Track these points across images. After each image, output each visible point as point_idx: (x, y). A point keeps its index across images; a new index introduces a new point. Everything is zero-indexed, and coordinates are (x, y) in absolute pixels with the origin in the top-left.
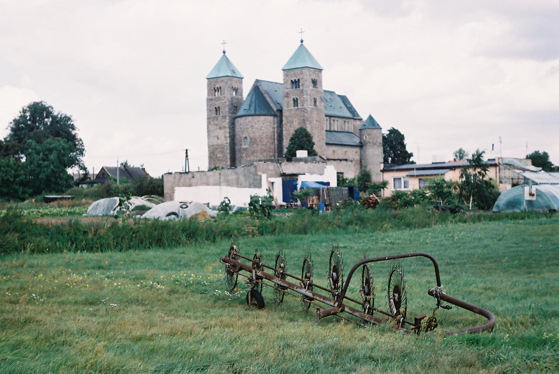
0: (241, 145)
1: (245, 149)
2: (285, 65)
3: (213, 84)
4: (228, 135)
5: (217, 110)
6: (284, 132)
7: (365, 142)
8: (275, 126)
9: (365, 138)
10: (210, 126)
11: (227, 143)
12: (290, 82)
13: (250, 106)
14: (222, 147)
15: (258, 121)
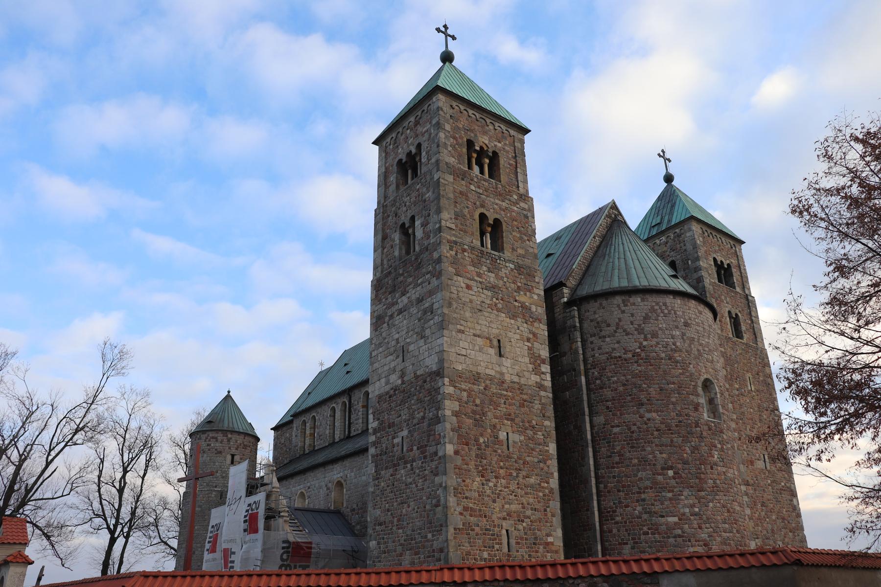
3: (463, 123)
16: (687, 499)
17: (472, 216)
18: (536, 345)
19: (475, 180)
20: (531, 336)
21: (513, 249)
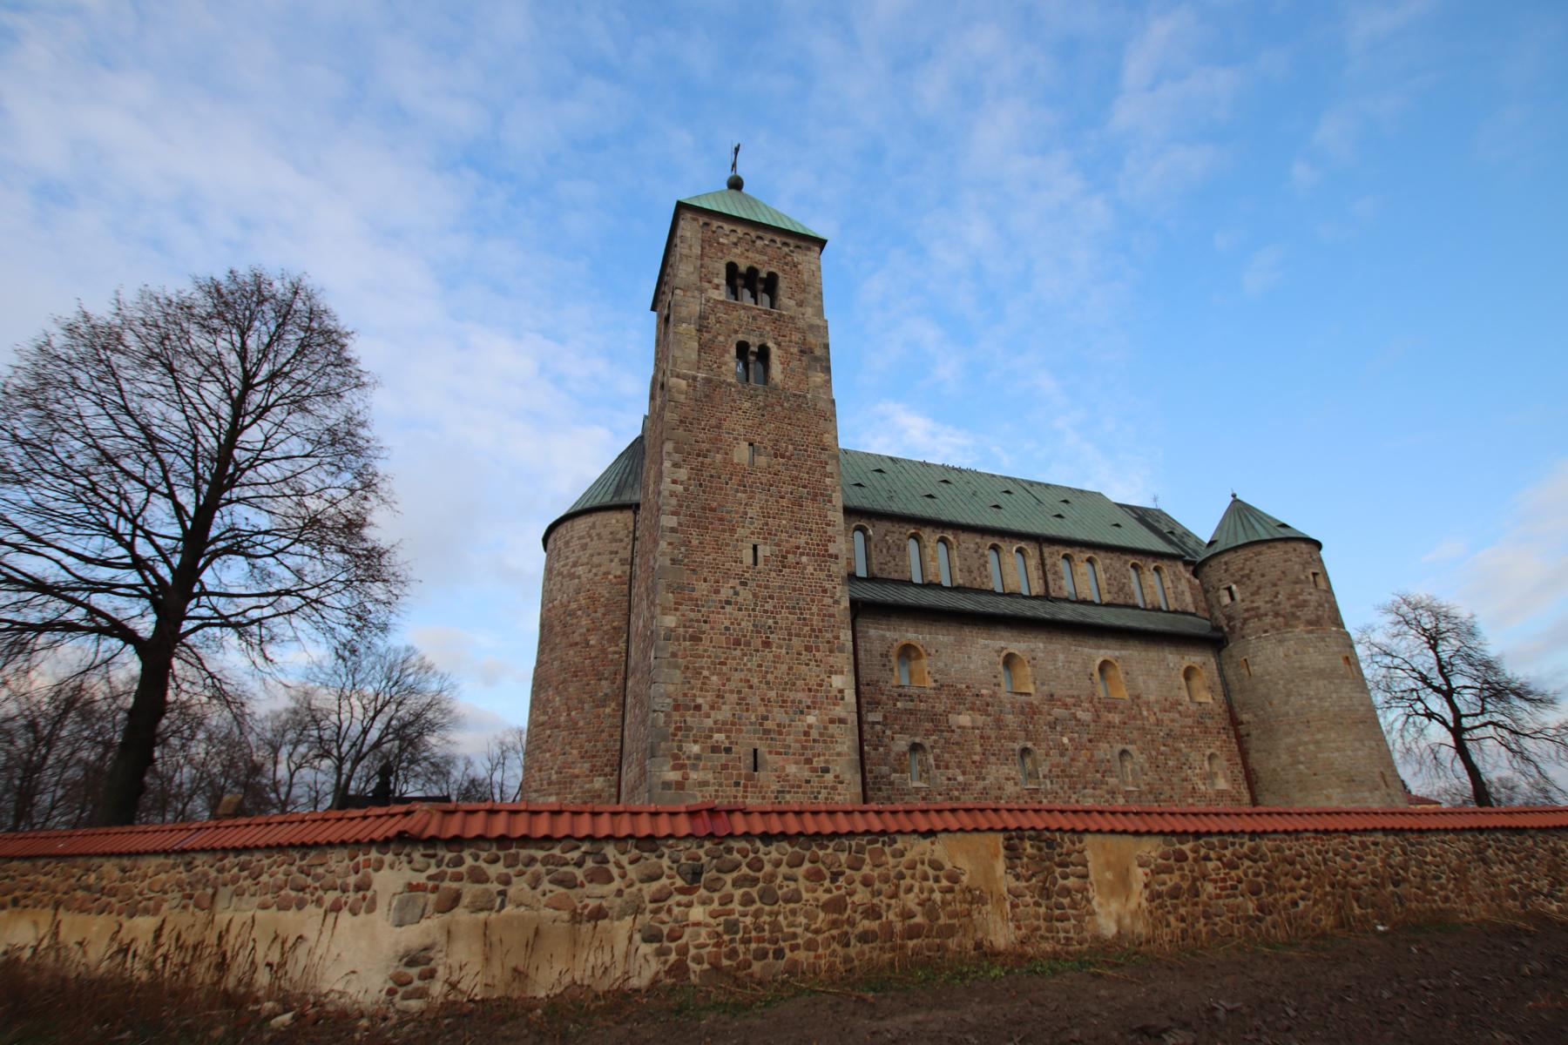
7: (1230, 618)
9: (1226, 600)
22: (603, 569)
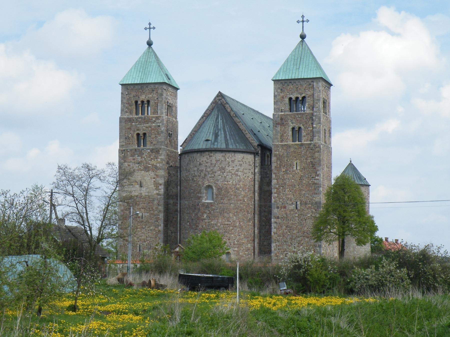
0: (199, 198)
1: (208, 206)
2: (279, 72)
3: (133, 94)
4: (162, 181)
5: (141, 138)
6: (274, 182)
8: (257, 170)
10: (126, 164)
11: (158, 194)
12: (287, 100)
13: (216, 136)
14: (149, 200)
15: (233, 161)
16: (192, 234)
17: (133, 137)
18: (158, 179)
19: (135, 120)
20: (155, 176)
21: (151, 143)
22: (247, 175)
